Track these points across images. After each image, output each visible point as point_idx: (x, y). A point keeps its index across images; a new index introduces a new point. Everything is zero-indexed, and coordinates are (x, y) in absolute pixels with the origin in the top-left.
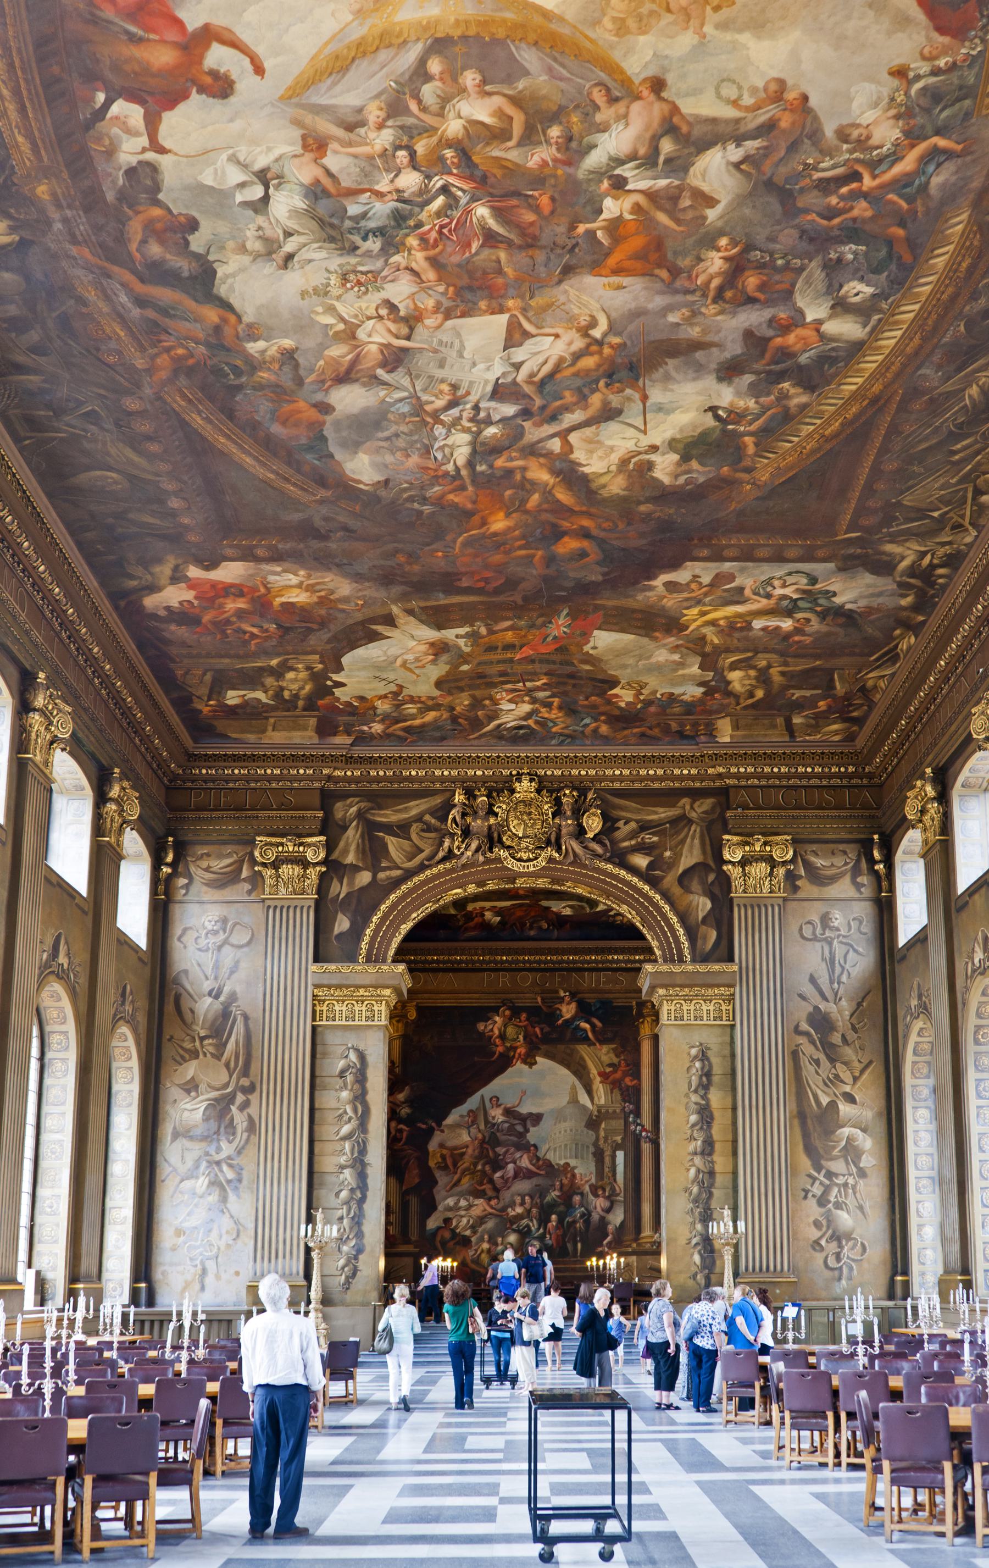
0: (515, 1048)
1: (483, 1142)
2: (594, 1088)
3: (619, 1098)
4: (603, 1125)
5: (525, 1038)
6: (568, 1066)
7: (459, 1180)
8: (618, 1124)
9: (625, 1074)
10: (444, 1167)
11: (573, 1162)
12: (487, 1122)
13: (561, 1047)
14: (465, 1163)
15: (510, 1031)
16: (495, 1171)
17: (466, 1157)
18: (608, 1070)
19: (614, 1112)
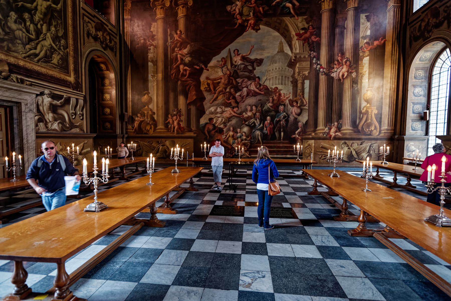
0: (248, 21)
1: (230, 76)
2: (293, 43)
3: (308, 49)
4: (298, 65)
5: (253, 15)
6: (278, 31)
7: (217, 97)
8: (306, 64)
9: (312, 34)
10: (209, 90)
11: (280, 87)
12: (232, 64)
13: (274, 19)
14: (220, 88)
15: (245, 10)
16: (236, 92)
17: (221, 84)
18: (302, 32)
19: (305, 57)
